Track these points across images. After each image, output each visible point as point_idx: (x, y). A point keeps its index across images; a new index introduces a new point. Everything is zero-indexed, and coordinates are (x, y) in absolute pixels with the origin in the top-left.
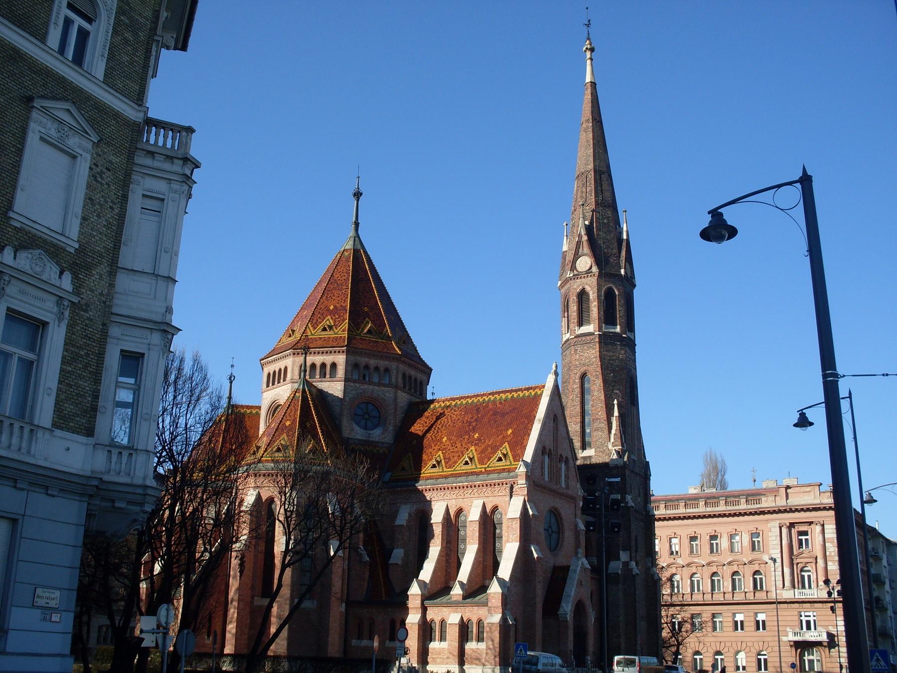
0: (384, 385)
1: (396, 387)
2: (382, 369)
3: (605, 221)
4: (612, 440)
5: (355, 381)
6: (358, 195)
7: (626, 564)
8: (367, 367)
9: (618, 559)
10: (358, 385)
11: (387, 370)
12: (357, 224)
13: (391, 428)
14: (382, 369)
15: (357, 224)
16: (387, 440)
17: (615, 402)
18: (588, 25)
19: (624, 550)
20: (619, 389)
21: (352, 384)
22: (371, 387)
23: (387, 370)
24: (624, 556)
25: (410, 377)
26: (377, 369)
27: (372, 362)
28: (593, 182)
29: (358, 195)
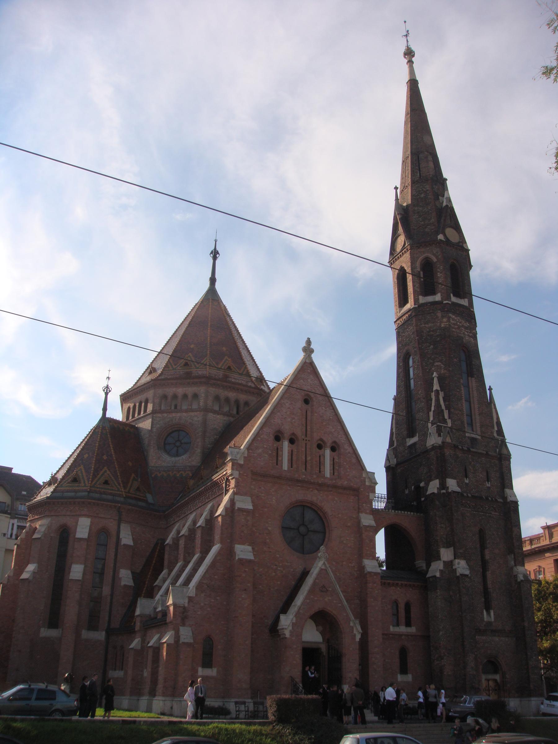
0: (192, 410)
1: (206, 410)
2: (190, 396)
3: (422, 196)
4: (431, 419)
5: (161, 412)
6: (215, 254)
7: (449, 564)
8: (175, 397)
9: (438, 558)
10: (165, 415)
11: (196, 396)
12: (213, 280)
13: (199, 451)
14: (190, 396)
15: (213, 280)
16: (194, 463)
17: (435, 374)
18: (406, 36)
19: (448, 546)
20: (441, 361)
21: (159, 415)
22: (179, 415)
23: (196, 396)
24: (446, 554)
25: (227, 400)
26: (185, 396)
27: (180, 391)
28: (410, 164)
29: (215, 254)
